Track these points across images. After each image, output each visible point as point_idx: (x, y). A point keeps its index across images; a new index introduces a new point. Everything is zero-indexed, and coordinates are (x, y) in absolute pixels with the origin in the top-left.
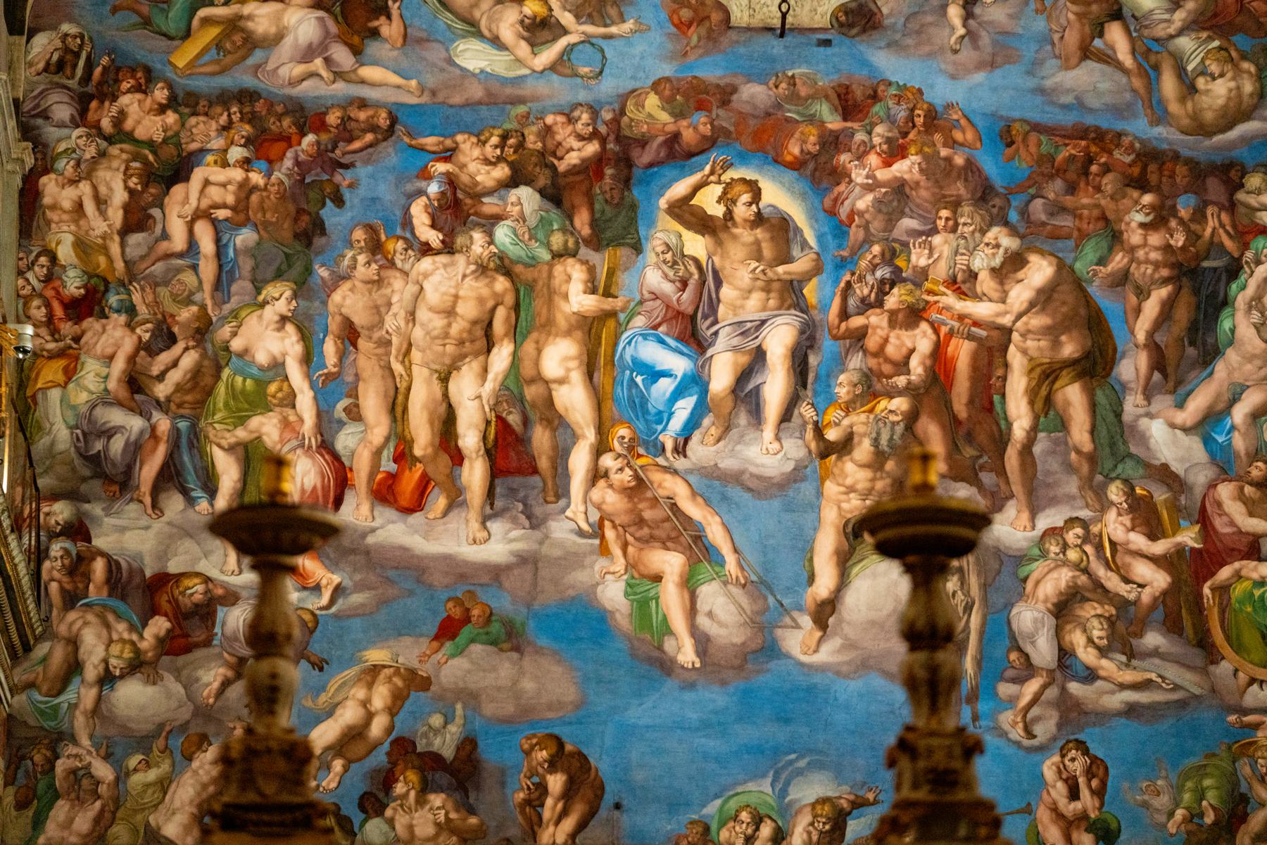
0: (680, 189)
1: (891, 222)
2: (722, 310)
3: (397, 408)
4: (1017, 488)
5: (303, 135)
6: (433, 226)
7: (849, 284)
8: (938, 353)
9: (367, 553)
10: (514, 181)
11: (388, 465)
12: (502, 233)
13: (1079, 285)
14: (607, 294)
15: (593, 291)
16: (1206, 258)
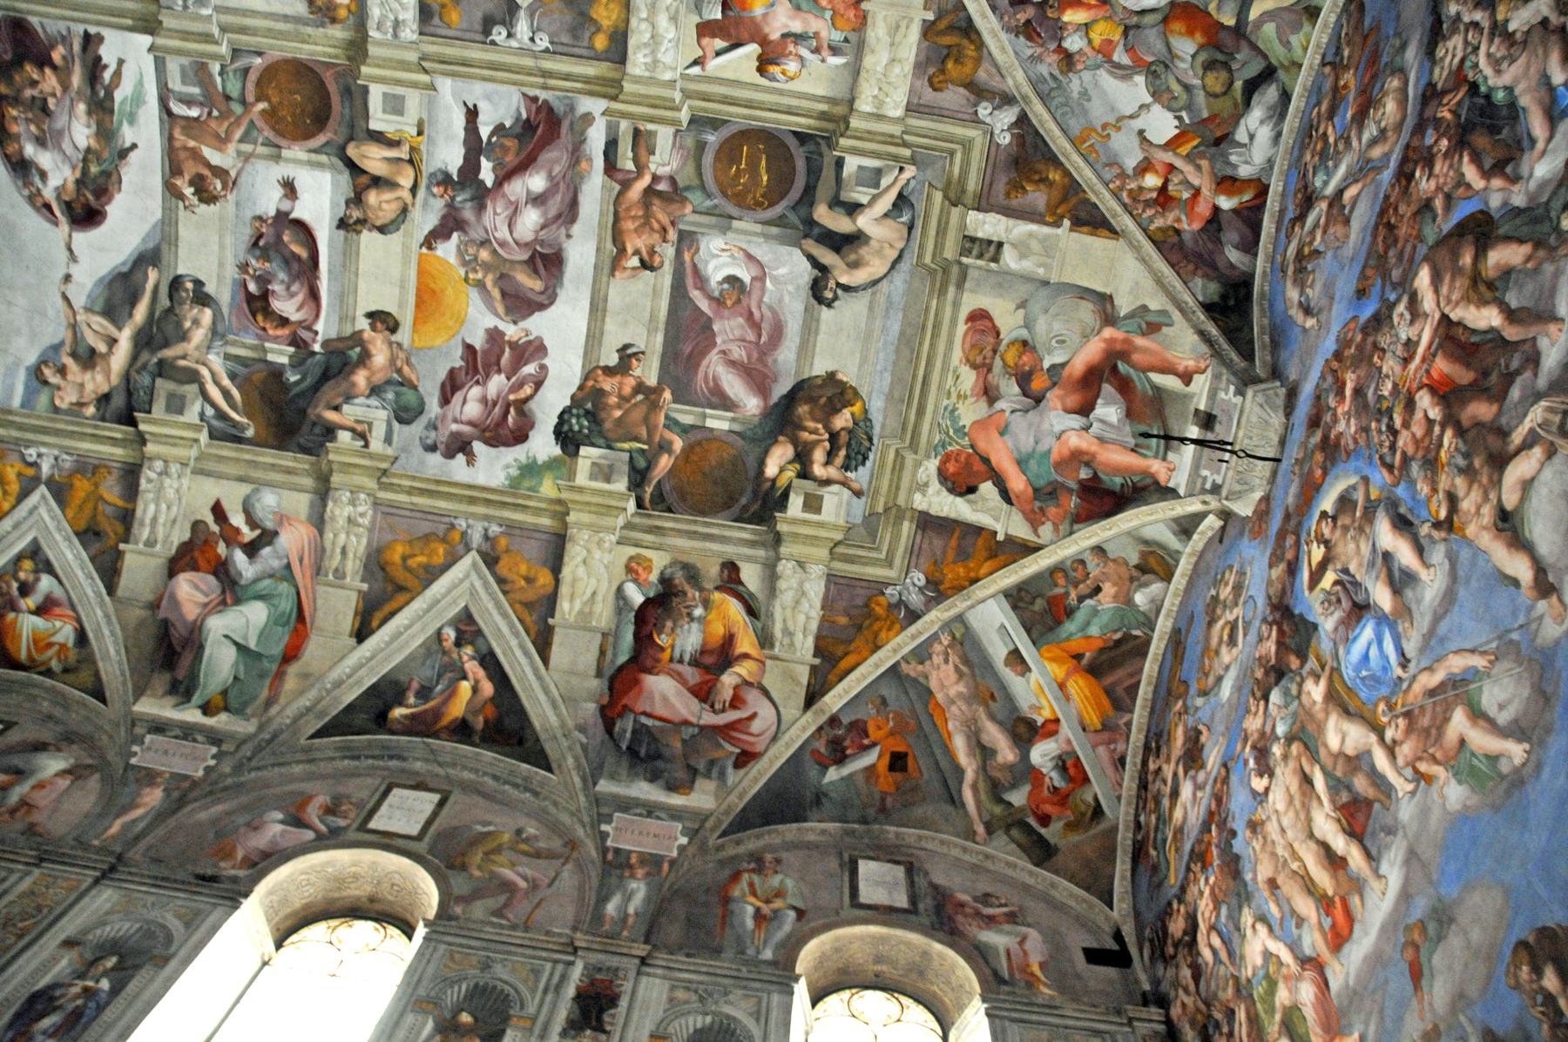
0: (1306, 575)
1: (1366, 406)
2: (1358, 577)
3: (1309, 887)
4: (1531, 332)
5: (1210, 831)
6: (1261, 776)
7: (1381, 458)
8: (1433, 390)
9: (1355, 992)
10: (1267, 701)
11: (1327, 922)
12: (1281, 730)
13: (1440, 243)
14: (1323, 668)
15: (1317, 678)
16: (1459, 116)
